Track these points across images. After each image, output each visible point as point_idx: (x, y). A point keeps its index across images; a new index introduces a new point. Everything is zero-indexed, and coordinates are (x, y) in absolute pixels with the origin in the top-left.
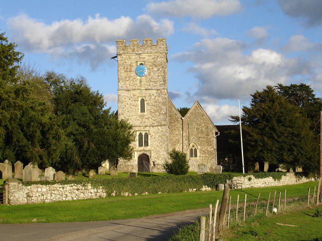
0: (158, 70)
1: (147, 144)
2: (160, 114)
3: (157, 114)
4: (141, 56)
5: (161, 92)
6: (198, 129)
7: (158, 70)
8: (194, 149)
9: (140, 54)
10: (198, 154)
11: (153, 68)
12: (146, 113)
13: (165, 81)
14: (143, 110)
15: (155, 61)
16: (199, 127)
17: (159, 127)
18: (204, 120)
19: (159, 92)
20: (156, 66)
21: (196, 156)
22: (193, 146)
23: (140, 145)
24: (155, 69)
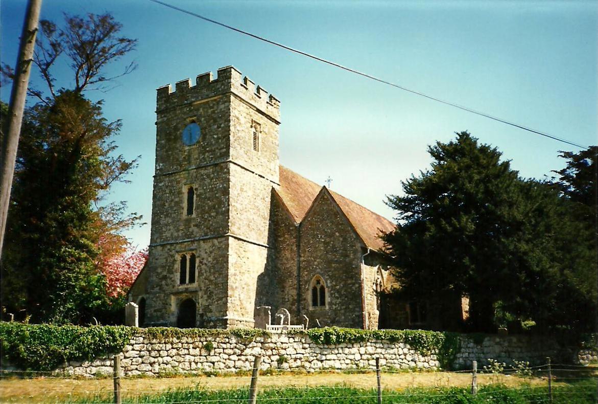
1: (192, 280)
2: (217, 213)
3: (212, 214)
6: (326, 244)
8: (318, 287)
10: (328, 299)
12: (194, 215)
14: (190, 211)
16: (328, 240)
17: (216, 241)
18: (338, 224)
19: (218, 168)
21: (323, 303)
22: (318, 282)
23: (183, 281)
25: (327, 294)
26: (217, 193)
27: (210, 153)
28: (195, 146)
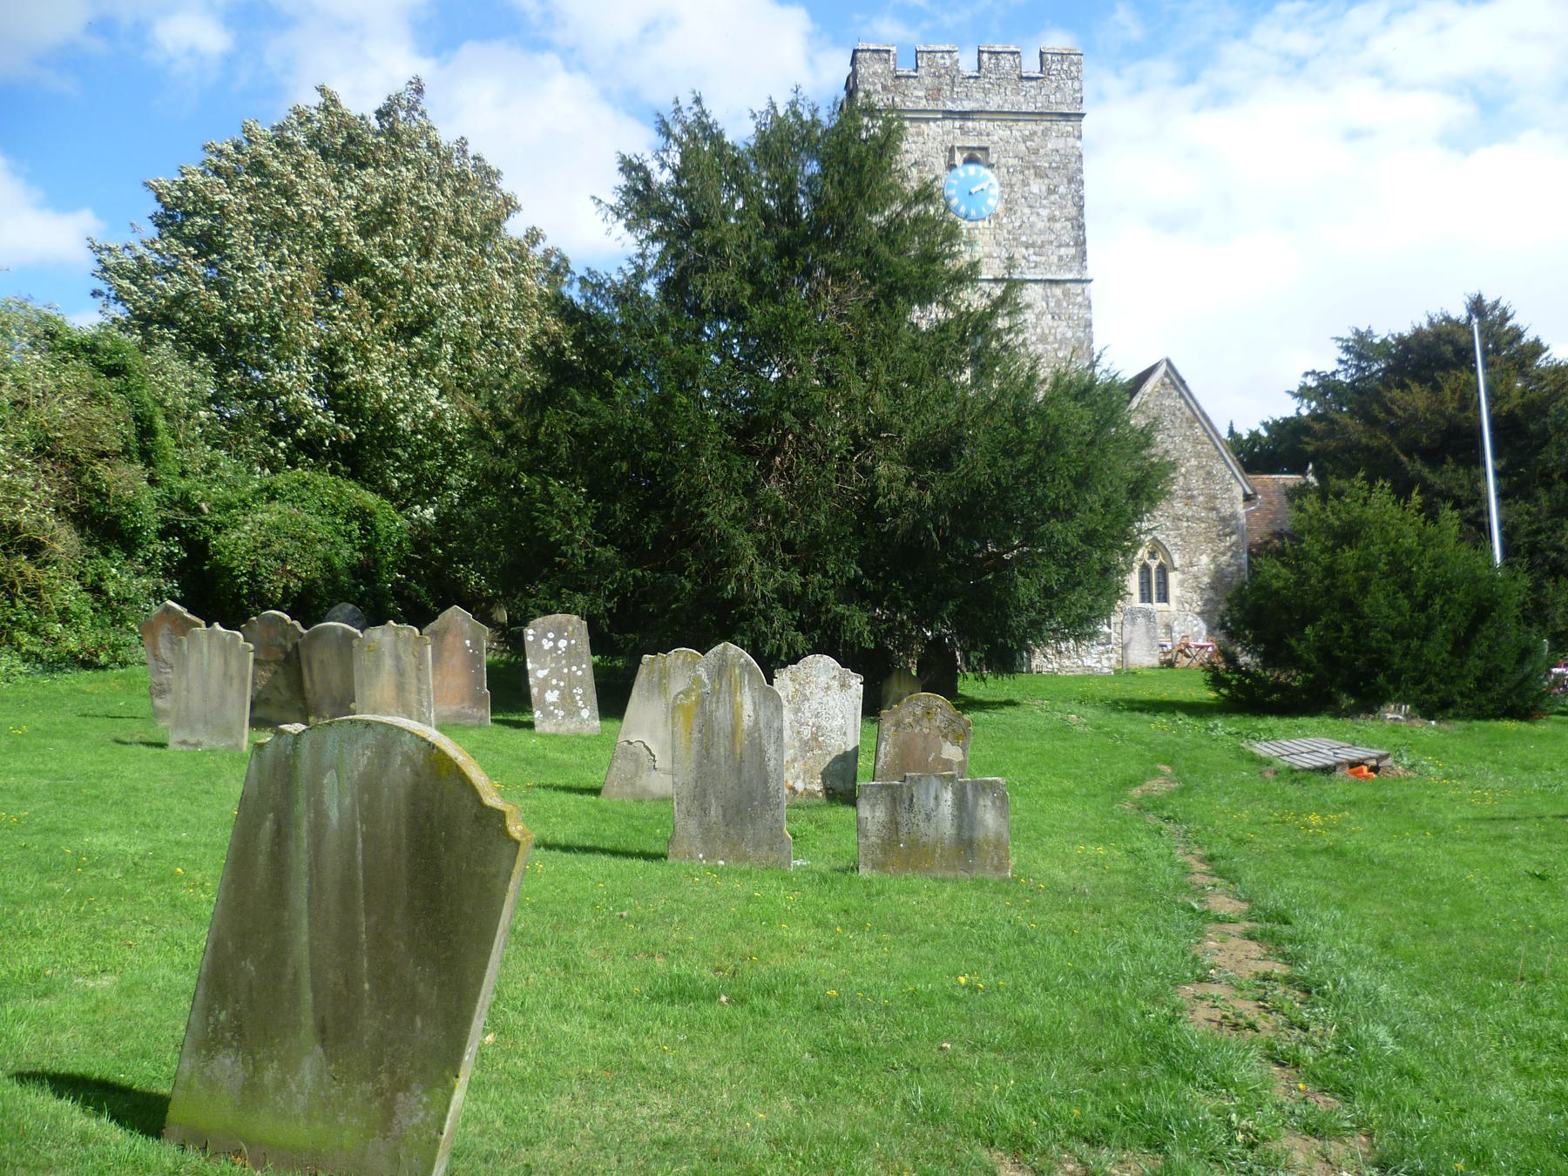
0: (1051, 191)
4: (970, 124)
5: (1066, 294)
7: (1051, 191)
8: (1154, 564)
9: (965, 115)
10: (1174, 590)
11: (1025, 183)
13: (1080, 243)
15: (1036, 152)
18: (1197, 441)
19: (1058, 291)
20: (1040, 175)
21: (1164, 597)
24: (1037, 187)
25: (1173, 578)
26: (1060, 349)
27: (1031, 251)
28: (986, 224)
